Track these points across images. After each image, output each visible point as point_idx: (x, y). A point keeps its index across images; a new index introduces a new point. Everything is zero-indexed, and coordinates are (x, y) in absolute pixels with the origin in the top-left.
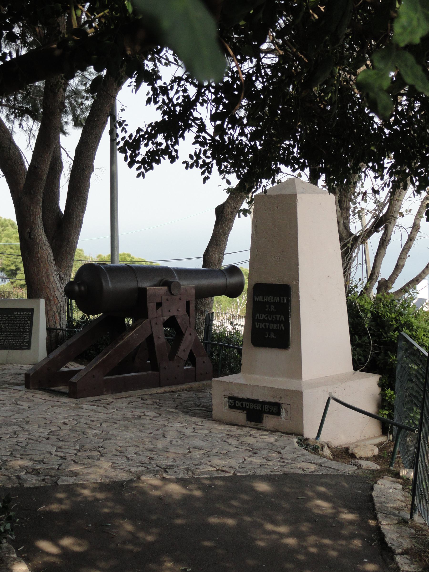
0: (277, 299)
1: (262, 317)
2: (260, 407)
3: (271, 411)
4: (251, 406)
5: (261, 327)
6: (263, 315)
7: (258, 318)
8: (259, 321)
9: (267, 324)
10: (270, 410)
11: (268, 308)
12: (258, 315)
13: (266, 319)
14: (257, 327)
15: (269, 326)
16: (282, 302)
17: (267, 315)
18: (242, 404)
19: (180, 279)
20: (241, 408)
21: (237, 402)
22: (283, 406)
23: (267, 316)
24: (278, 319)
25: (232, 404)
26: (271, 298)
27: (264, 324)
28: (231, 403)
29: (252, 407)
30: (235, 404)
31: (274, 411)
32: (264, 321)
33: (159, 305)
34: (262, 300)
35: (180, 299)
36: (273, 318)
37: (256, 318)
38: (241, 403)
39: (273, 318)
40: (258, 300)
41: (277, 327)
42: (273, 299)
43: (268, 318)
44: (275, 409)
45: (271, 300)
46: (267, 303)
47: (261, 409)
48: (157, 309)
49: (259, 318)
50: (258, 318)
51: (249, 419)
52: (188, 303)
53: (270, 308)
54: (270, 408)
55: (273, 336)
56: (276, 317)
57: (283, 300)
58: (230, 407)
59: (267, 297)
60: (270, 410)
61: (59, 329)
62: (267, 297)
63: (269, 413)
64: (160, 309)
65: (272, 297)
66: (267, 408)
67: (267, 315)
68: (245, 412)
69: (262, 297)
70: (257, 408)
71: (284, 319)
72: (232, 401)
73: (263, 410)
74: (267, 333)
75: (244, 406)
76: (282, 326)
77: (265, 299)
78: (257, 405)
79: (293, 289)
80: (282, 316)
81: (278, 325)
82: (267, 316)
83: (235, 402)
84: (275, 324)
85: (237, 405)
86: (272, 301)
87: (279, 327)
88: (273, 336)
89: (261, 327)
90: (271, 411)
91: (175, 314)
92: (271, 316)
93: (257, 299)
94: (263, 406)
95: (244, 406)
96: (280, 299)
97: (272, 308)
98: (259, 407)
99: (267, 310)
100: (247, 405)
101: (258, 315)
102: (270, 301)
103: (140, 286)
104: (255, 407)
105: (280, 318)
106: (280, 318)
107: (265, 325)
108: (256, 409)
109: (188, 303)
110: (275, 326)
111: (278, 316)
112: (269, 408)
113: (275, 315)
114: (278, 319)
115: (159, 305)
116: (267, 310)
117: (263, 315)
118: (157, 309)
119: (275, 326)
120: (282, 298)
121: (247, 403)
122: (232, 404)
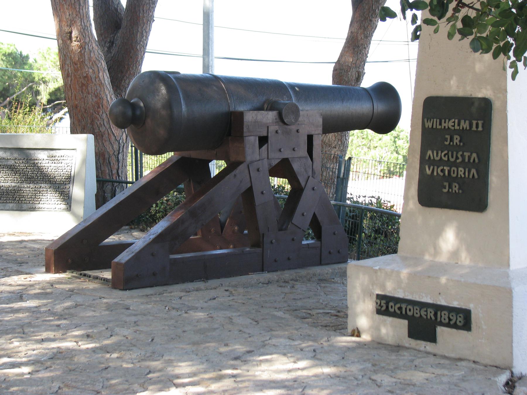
0: (465, 125)
1: (437, 156)
3: (452, 323)
4: (417, 312)
5: (435, 174)
6: (440, 152)
8: (431, 162)
10: (450, 320)
12: (430, 152)
13: (446, 159)
15: (449, 172)
16: (474, 128)
18: (400, 308)
19: (298, 100)
21: (391, 304)
23: (447, 154)
24: (467, 160)
25: (382, 307)
26: (454, 122)
27: (441, 168)
29: (418, 315)
30: (387, 307)
31: (458, 323)
36: (457, 158)
37: (427, 158)
38: (398, 305)
39: (457, 158)
40: (430, 127)
41: (464, 173)
42: (459, 125)
44: (459, 319)
45: (454, 126)
46: (447, 130)
47: (433, 318)
48: (260, 146)
49: (432, 158)
51: (413, 333)
52: (310, 138)
53: (452, 140)
54: (451, 317)
56: (462, 156)
57: (477, 126)
60: (450, 320)
61: (117, 182)
63: (448, 325)
64: (264, 147)
65: (456, 121)
67: (446, 152)
68: (406, 322)
69: (438, 120)
70: (427, 315)
72: (383, 302)
73: (439, 320)
74: (446, 184)
75: (404, 312)
76: (473, 171)
77: (443, 124)
78: (426, 311)
79: (496, 105)
80: (474, 155)
81: (467, 170)
83: (387, 304)
84: (460, 169)
85: (392, 310)
86: (457, 127)
87: (469, 175)
88: (456, 188)
89: (435, 174)
90: (452, 323)
91: (287, 154)
92: (455, 153)
93: (429, 124)
94: (439, 313)
95: (404, 312)
96: (471, 125)
97: (457, 140)
99: (447, 143)
100: (410, 310)
101: (430, 152)
102: (453, 128)
103: (232, 109)
104: (423, 313)
105: (469, 158)
106: (469, 158)
107: (442, 171)
108: (425, 317)
109: (310, 138)
111: (467, 154)
112: (449, 317)
113: (460, 153)
114: (467, 160)
117: (440, 152)
118: (260, 146)
120: (474, 122)
121: (409, 307)
122: (382, 307)
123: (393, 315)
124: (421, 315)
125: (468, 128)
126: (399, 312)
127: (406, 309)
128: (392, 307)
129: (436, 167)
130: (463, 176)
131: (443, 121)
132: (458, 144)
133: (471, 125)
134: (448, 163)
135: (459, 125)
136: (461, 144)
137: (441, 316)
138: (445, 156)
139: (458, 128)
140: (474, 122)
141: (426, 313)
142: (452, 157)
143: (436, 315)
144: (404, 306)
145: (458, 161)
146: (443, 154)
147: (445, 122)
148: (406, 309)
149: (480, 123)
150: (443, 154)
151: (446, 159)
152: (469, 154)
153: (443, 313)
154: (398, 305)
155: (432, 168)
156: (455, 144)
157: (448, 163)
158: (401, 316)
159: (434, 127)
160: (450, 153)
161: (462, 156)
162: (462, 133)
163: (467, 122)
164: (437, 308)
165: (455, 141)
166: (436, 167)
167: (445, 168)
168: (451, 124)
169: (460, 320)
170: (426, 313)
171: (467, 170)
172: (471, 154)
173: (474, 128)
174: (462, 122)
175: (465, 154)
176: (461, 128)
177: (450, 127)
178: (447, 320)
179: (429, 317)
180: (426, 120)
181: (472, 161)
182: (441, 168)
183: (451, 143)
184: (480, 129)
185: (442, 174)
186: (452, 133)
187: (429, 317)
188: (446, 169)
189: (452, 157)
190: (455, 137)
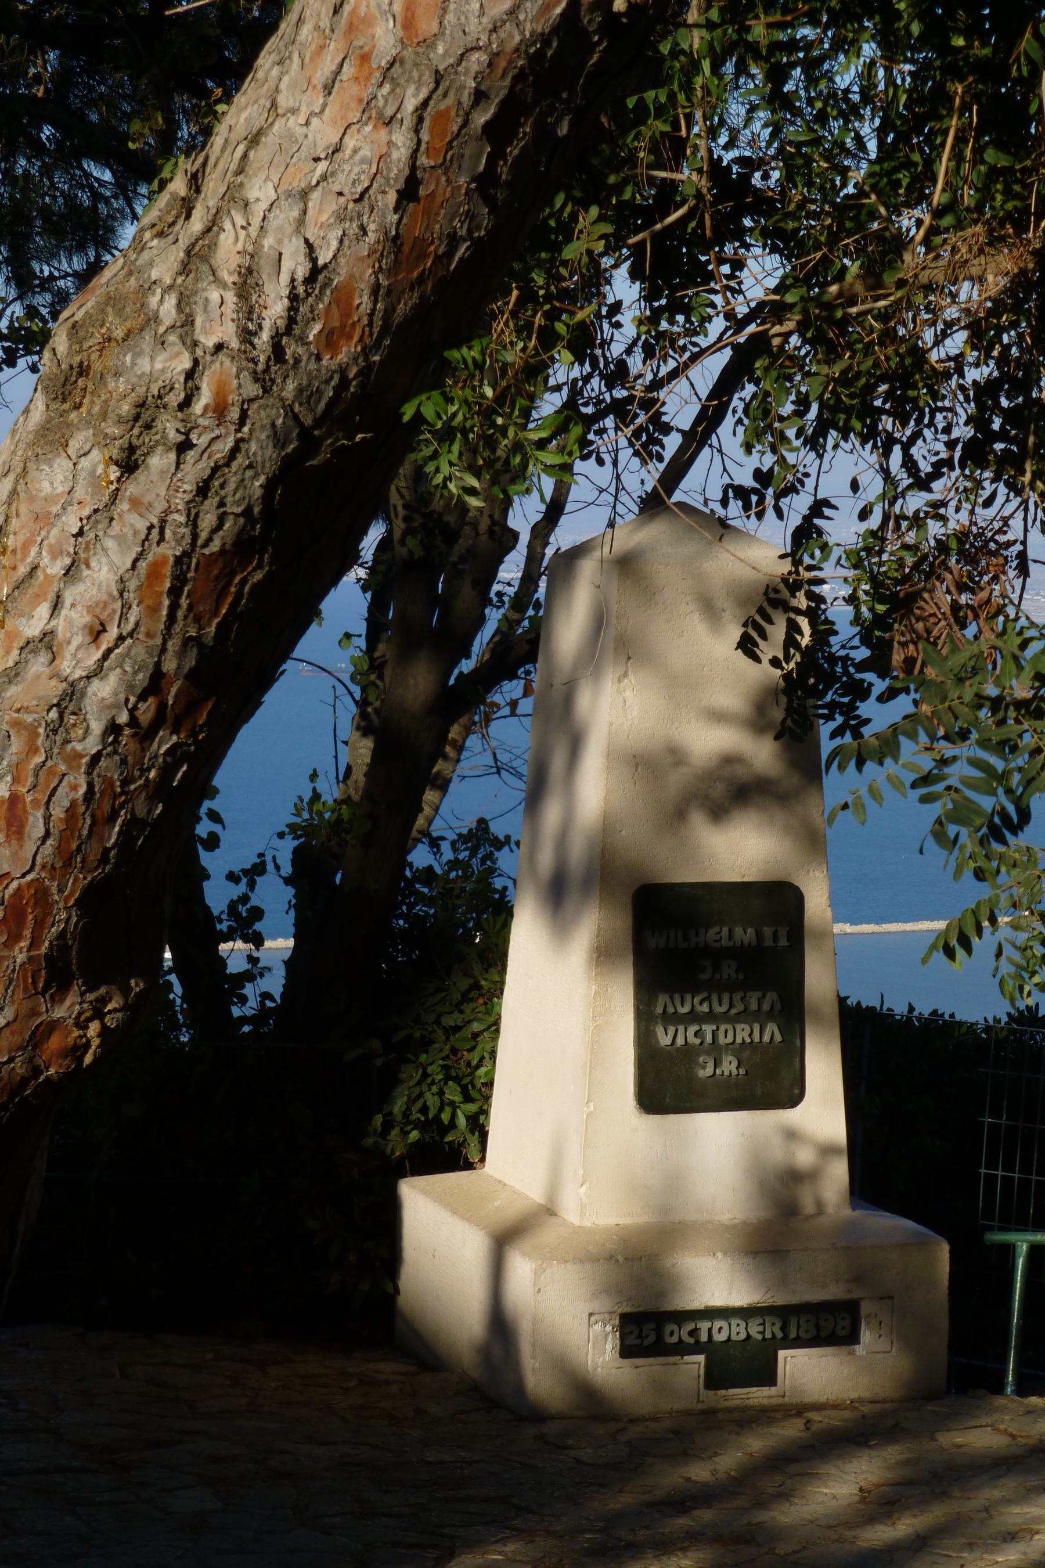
9: (708, 1029)
15: (714, 1034)
17: (705, 995)
29: (743, 1336)
30: (660, 1338)
41: (750, 1035)
49: (671, 1010)
55: (729, 1066)
57: (775, 938)
62: (702, 931)
67: (705, 995)
70: (763, 1333)
75: (704, 1338)
82: (708, 999)
84: (739, 1027)
88: (729, 1066)
89: (680, 1041)
93: (654, 942)
102: (717, 945)
104: (754, 1330)
121: (717, 1324)
124: (749, 1337)
127: (710, 1330)
129: (681, 1029)
130: (748, 1040)
136: (741, 976)
139: (731, 944)
141: (761, 1328)
145: (733, 1011)
146: (697, 1000)
147: (697, 934)
148: (710, 1330)
150: (697, 1000)
152: (759, 994)
154: (691, 1326)
155: (671, 1030)
163: (750, 931)
166: (681, 1029)
167: (704, 1027)
170: (761, 1328)
175: (749, 994)
179: (768, 1335)
181: (766, 1007)
182: (696, 1028)
183: (717, 976)
185: (698, 1041)
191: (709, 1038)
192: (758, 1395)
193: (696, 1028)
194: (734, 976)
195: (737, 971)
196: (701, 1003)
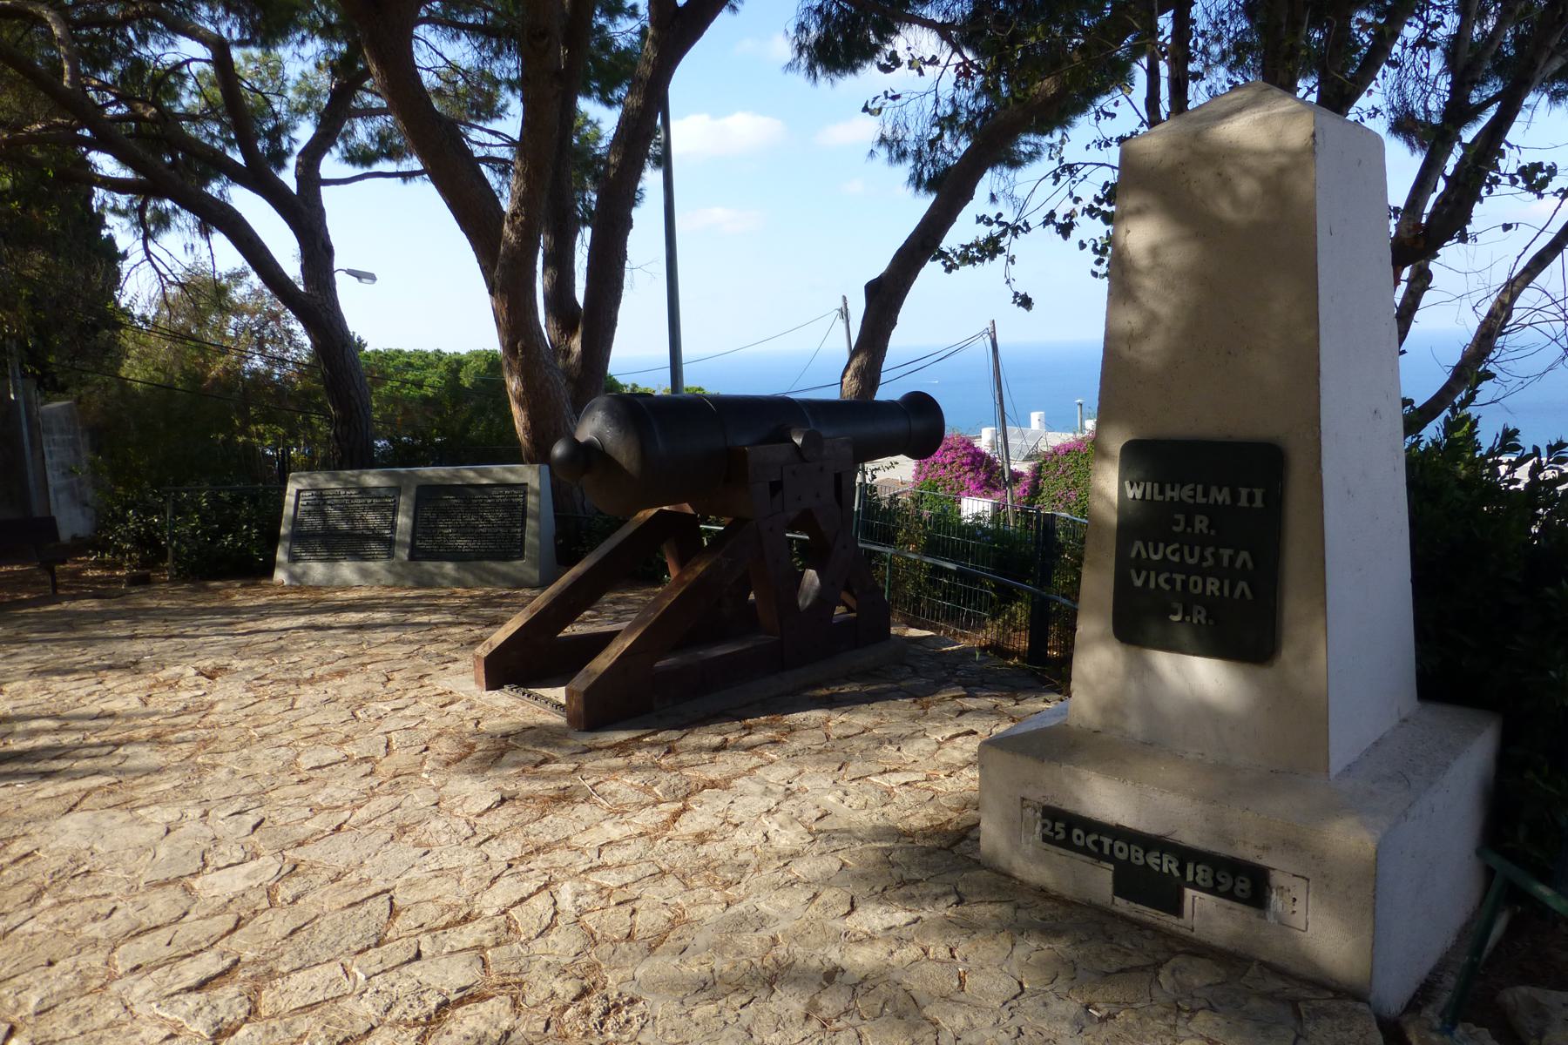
0: (1222, 496)
2: (1174, 867)
3: (1221, 888)
6: (1161, 546)
7: (1139, 553)
8: (1141, 565)
9: (1179, 578)
11: (1182, 524)
13: (1176, 559)
14: (1139, 583)
15: (1185, 584)
16: (1243, 502)
17: (1176, 546)
18: (1098, 843)
20: (1098, 855)
21: (1076, 832)
22: (1277, 879)
26: (1195, 490)
28: (1053, 829)
29: (1141, 862)
31: (1237, 892)
32: (1164, 565)
33: (776, 487)
34: (1157, 498)
35: (822, 469)
37: (1133, 554)
38: (1094, 837)
39: (1202, 558)
40: (1139, 496)
41: (1221, 589)
43: (1182, 556)
44: (1239, 886)
45: (1194, 497)
46: (1180, 505)
47: (1177, 874)
49: (1144, 555)
50: (1139, 553)
53: (1189, 522)
57: (1251, 498)
58: (1046, 839)
59: (1177, 486)
60: (1216, 883)
62: (1177, 486)
65: (1200, 488)
66: (1209, 876)
67: (1176, 546)
70: (1161, 866)
71: (1250, 565)
72: (1059, 826)
73: (1190, 878)
75: (1107, 851)
76: (1243, 585)
77: (1169, 494)
80: (1244, 555)
81: (1227, 583)
82: (1180, 550)
84: (1210, 580)
86: (1200, 500)
89: (1152, 585)
92: (1197, 550)
94: (1190, 867)
95: (1107, 851)
96: (1235, 496)
97: (1201, 523)
98: (1169, 865)
99: (1175, 529)
100: (1121, 850)
104: (1152, 860)
105: (1232, 560)
110: (1212, 586)
112: (1214, 878)
113: (1210, 550)
115: (776, 487)
116: (1175, 529)
117: (1161, 546)
119: (1212, 586)
120: (1244, 492)
121: (1118, 844)
123: (1084, 850)
125: (1228, 502)
126: (1095, 849)
127: (1112, 846)
128: (1079, 837)
129: (1153, 574)
131: (1168, 487)
132: (1205, 531)
133: (1235, 496)
134: (1182, 567)
135: (1206, 494)
136: (1213, 532)
137: (1195, 874)
138: (1173, 553)
140: (1244, 492)
142: (1192, 556)
143: (1182, 869)
144: (1107, 841)
146: (1169, 550)
149: (1258, 493)
150: (1169, 550)
151: (1176, 559)
153: (1200, 868)
154: (1095, 837)
156: (1197, 531)
157: (1182, 567)
158: (1099, 855)
159: (1148, 497)
160: (1186, 550)
161: (1215, 555)
162: (1212, 511)
163: (1226, 490)
164: (1186, 855)
165: (1198, 526)
166: (1153, 574)
168: (1186, 492)
169: (1244, 885)
171: (1227, 583)
172: (1237, 553)
173: (1243, 502)
174: (1214, 490)
175: (1221, 551)
176: (1212, 501)
177: (1184, 498)
178: (1210, 883)
180: (1127, 484)
181: (1238, 564)
182: (1166, 575)
184: (1258, 503)
185: (1167, 587)
186: (1190, 511)
187: (1165, 870)
188: (1179, 578)
189: (1192, 556)
190: (1198, 518)
191: (1179, 586)
192: (1167, 920)
193: (1166, 575)
194: (1205, 531)
195: (1209, 527)
196: (1173, 553)
